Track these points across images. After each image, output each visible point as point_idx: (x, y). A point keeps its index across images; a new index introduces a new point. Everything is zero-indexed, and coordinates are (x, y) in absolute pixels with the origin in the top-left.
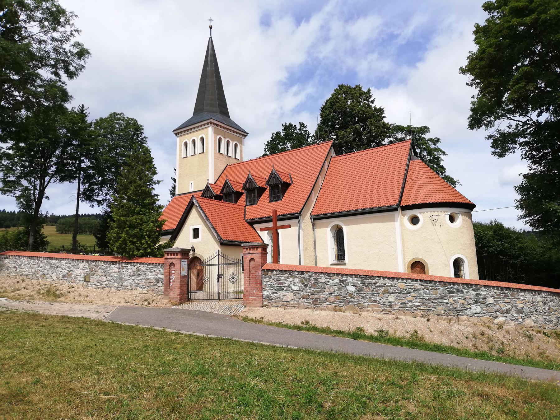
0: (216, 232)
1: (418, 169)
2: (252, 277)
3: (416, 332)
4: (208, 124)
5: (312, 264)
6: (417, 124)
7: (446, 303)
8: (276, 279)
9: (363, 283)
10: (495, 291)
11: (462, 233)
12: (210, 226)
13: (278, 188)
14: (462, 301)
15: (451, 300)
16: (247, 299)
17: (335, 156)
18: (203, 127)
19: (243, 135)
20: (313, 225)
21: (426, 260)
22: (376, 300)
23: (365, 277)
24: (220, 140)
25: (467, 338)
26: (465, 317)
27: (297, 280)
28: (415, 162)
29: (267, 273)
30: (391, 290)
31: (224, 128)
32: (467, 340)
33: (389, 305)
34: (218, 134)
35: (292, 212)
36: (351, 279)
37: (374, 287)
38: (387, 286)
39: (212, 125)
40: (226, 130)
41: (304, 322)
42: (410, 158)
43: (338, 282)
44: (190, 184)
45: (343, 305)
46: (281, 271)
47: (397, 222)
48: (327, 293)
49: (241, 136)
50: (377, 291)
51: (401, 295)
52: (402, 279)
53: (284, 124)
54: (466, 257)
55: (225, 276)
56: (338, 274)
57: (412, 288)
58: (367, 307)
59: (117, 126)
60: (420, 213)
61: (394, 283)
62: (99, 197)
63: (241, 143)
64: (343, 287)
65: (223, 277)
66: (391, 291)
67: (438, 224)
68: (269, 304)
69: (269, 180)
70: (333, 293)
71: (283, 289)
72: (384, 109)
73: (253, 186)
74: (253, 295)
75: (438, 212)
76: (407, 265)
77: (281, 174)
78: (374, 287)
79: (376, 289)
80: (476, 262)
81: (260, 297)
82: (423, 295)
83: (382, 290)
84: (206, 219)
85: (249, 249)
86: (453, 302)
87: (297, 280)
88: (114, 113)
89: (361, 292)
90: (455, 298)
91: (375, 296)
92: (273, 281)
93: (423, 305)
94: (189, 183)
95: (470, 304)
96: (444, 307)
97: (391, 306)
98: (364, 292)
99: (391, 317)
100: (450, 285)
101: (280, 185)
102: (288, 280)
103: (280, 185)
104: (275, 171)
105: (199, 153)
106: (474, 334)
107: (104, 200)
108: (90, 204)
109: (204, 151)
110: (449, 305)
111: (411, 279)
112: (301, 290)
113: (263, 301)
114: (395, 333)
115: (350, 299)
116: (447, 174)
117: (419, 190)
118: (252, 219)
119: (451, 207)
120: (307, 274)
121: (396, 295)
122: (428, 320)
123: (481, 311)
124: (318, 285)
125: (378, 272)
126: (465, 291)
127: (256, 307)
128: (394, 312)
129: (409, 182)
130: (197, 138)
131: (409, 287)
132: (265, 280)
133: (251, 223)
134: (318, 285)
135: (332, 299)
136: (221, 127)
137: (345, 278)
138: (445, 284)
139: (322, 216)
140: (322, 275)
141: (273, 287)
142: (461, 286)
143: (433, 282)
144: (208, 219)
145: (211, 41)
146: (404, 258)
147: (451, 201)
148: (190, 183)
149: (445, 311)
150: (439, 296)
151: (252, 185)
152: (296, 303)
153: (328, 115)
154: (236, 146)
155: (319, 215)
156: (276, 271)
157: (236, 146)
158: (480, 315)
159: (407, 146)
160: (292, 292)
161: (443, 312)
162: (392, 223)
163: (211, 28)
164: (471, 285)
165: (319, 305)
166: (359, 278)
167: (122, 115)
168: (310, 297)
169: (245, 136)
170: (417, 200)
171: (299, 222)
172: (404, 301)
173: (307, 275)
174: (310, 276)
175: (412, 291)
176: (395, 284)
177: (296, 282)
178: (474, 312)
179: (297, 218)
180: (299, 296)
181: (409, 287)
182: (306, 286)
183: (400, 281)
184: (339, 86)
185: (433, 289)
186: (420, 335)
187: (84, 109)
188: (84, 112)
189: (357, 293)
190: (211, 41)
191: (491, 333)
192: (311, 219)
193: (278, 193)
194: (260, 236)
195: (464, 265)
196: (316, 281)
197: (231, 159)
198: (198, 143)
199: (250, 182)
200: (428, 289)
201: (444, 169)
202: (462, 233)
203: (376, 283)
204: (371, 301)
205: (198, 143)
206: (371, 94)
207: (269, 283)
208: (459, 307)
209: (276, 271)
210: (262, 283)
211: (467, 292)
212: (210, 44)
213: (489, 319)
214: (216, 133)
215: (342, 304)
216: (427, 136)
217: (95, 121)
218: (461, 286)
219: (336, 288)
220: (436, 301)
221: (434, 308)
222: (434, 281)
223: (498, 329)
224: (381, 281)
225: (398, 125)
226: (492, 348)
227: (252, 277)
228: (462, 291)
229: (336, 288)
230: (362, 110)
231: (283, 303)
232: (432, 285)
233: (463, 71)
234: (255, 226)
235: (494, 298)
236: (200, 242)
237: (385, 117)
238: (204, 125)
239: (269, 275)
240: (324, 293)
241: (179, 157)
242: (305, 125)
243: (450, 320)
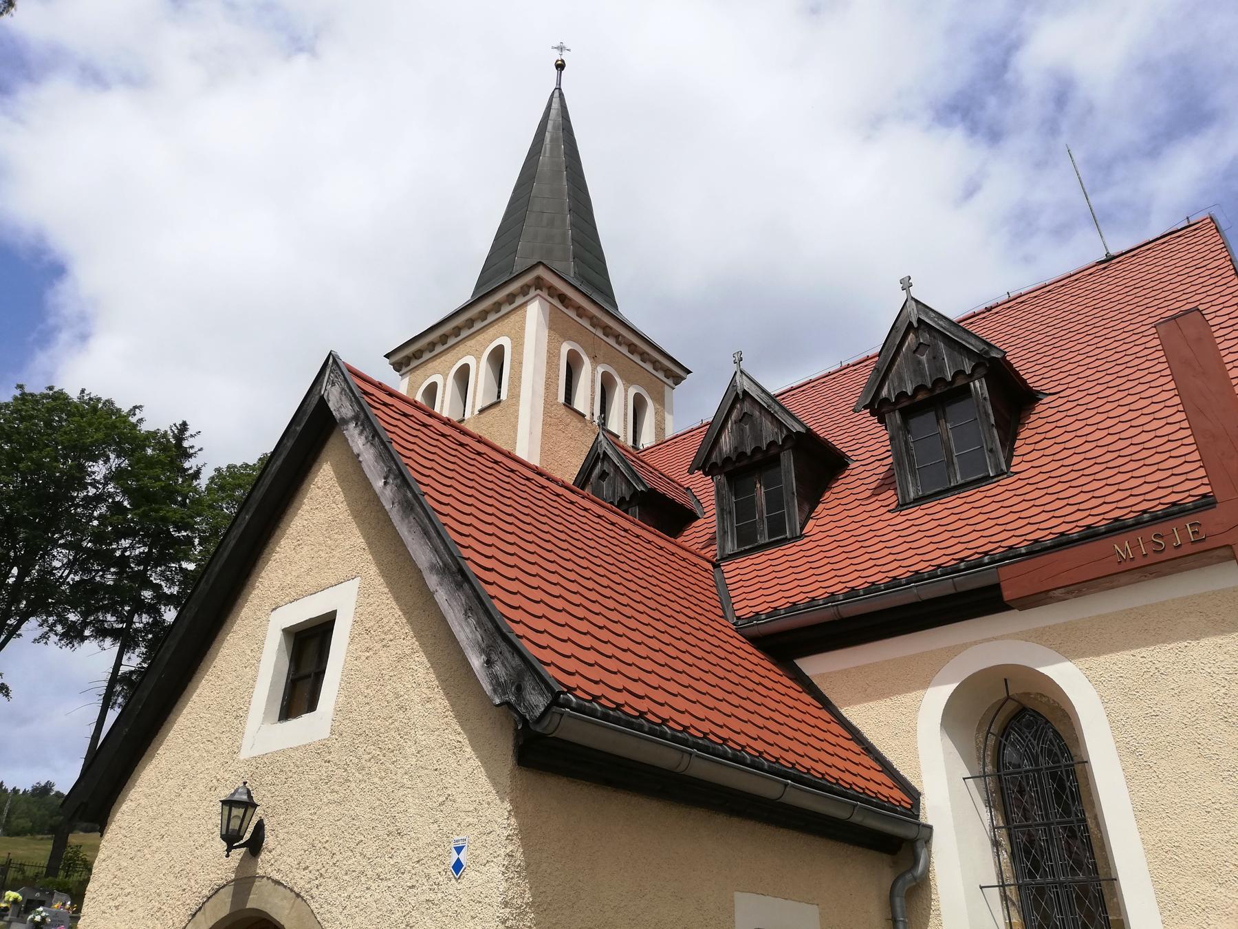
0: (479, 606)
4: (524, 291)
19: (668, 373)
39: (545, 294)
40: (600, 333)
49: (660, 375)
63: (660, 400)
73: (769, 432)
105: (478, 407)
109: (504, 396)
130: (478, 359)
136: (580, 311)
144: (412, 503)
151: (757, 435)
163: (560, 66)
169: (678, 380)
187: (187, 434)
188: (186, 444)
194: (869, 749)
198: (480, 374)
214: (557, 328)
217: (213, 473)
234: (813, 666)
236: (321, 750)
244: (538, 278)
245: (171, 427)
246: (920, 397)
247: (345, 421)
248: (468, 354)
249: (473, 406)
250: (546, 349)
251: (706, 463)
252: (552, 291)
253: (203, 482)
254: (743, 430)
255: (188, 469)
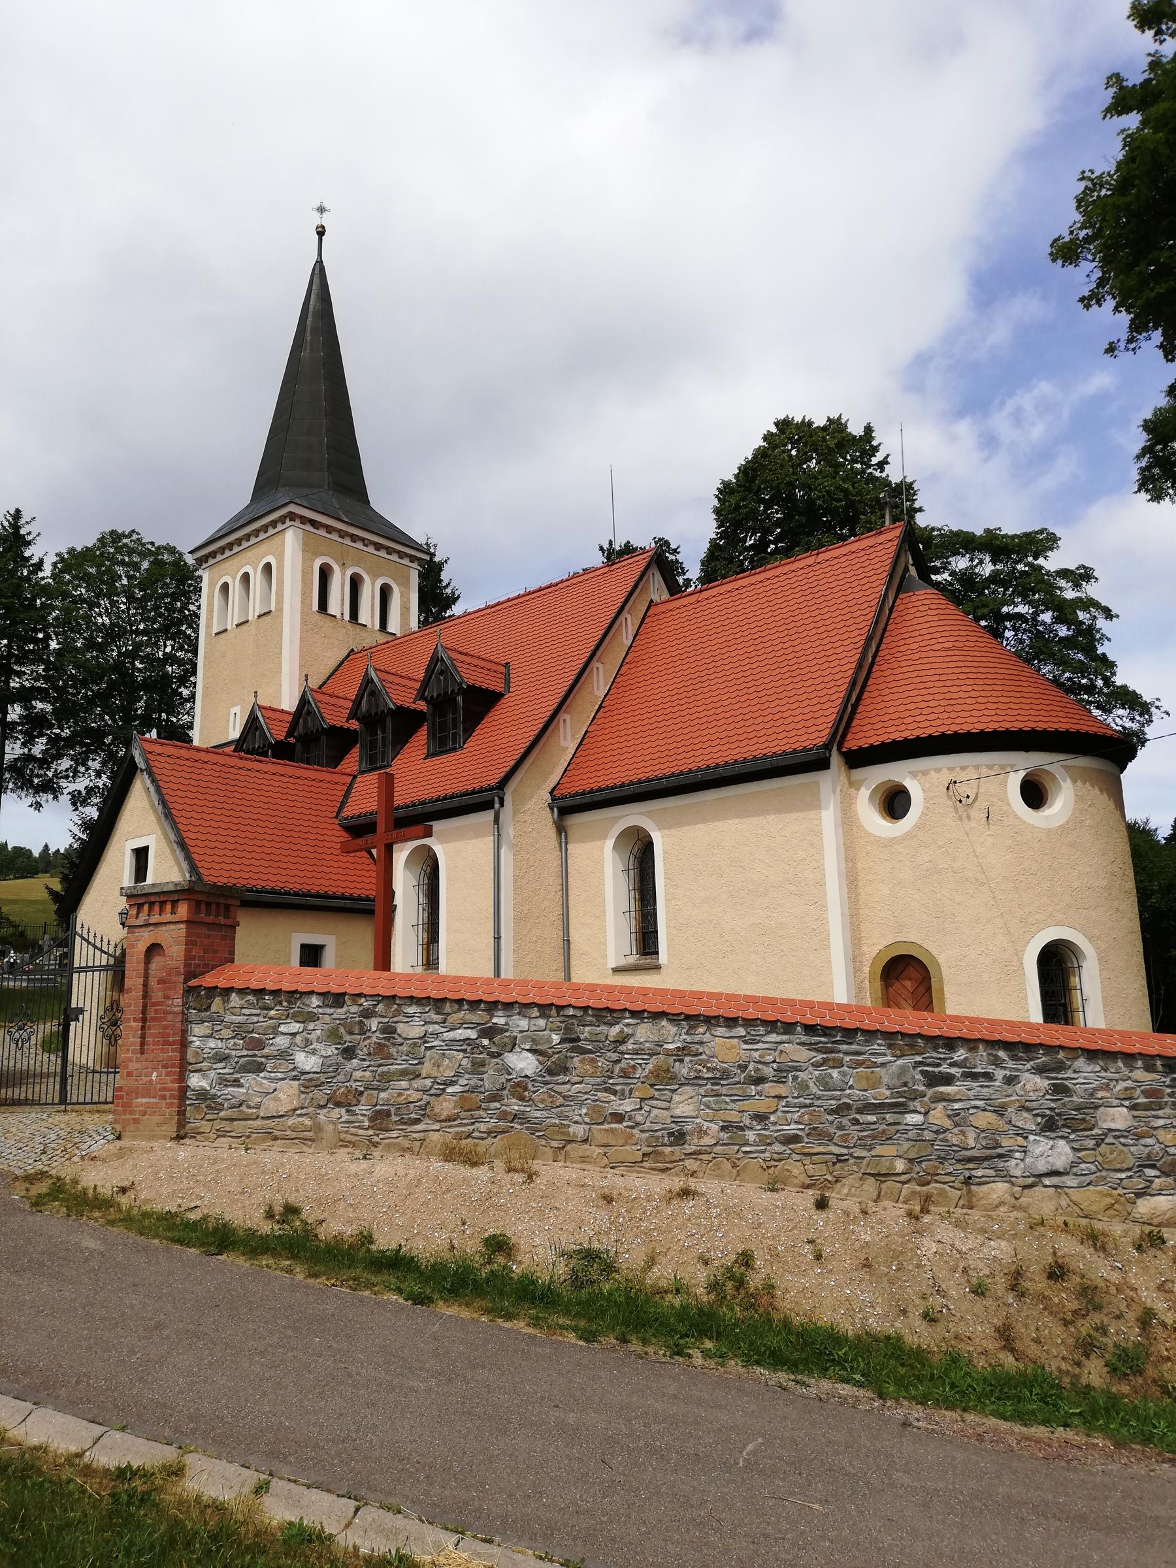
1: (921, 620)
2: (154, 1019)
3: (746, 1259)
4: (282, 520)
5: (548, 972)
6: (1012, 526)
7: (916, 1126)
8: (240, 1026)
9: (571, 1039)
10: (1140, 1074)
11: (1072, 845)
12: (172, 837)
13: (455, 711)
14: (984, 1119)
15: (938, 1115)
16: (127, 1106)
17: (666, 596)
18: (271, 531)
20: (561, 829)
21: (934, 952)
22: (620, 1110)
23: (579, 1013)
24: (325, 574)
25: (979, 1291)
26: (1001, 1187)
27: (317, 1030)
28: (914, 598)
29: (205, 1002)
30: (683, 1070)
31: (343, 534)
32: (979, 1305)
33: (671, 1134)
34: (317, 554)
35: (477, 786)
36: (524, 1023)
37: (615, 1057)
38: (668, 1053)
39: (297, 523)
40: (348, 541)
41: (278, 1209)
42: (898, 584)
43: (473, 1034)
44: (232, 716)
45: (489, 1133)
46: (259, 993)
47: (827, 808)
48: (428, 1082)
49: (406, 562)
50: (625, 1074)
51: (724, 1090)
52: (731, 1022)
53: (606, 546)
54: (1091, 939)
55: (87, 1015)
56: (475, 1004)
57: (769, 1058)
58: (585, 1141)
59: (120, 570)
60: (914, 774)
61: (697, 1038)
62: (78, 780)
64: (492, 1055)
65: (81, 1017)
66: (685, 1071)
67: (978, 813)
68: (205, 1126)
69: (425, 683)
70: (452, 1083)
71: (260, 1068)
72: (916, 486)
74: (147, 1091)
75: (977, 767)
76: (866, 969)
77: (468, 659)
78: (615, 1057)
79: (623, 1064)
80: (1139, 959)
81: (172, 1097)
82: (814, 1089)
83: (650, 1066)
84: (168, 813)
85: (146, 907)
86: (948, 1123)
87: (317, 1030)
88: (113, 532)
89: (561, 1078)
90: (956, 1106)
91: (615, 1093)
92: (227, 1033)
93: (816, 1133)
94: (229, 714)
95: (1023, 1134)
96: (906, 1145)
97: (679, 1138)
98: (577, 1079)
99: (659, 1184)
100: (935, 1049)
101: (459, 699)
102: (282, 1029)
103: (459, 699)
104: (445, 648)
106: (1018, 1274)
107: (90, 791)
108: (30, 800)
110: (928, 1135)
111: (764, 1022)
112: (330, 1070)
113: (182, 1113)
114: (651, 1261)
115: (515, 1106)
116: (1119, 680)
117: (911, 693)
118: (359, 816)
119: (1027, 749)
120: (355, 1002)
121: (702, 1091)
122: (822, 1204)
123: (1073, 1164)
124: (393, 1050)
125: (753, 1000)
126: (1000, 1074)
127: (153, 1138)
128: (691, 1164)
129: (883, 668)
130: (255, 570)
131: (756, 1055)
132: (198, 1029)
133: (360, 829)
134: (393, 1050)
135: (446, 1106)
136: (329, 529)
137: (499, 1020)
138: (912, 1046)
139: (586, 799)
140: (411, 1010)
141: (226, 1058)
142: (982, 1051)
143: (859, 1037)
145: (319, 271)
146: (855, 941)
147: (1027, 726)
148: (233, 710)
149: (910, 1161)
150: (883, 1094)
151: (377, 707)
152: (307, 1122)
153: (737, 508)
154: (385, 592)
155: (577, 794)
156: (242, 992)
157: (385, 592)
158: (1069, 1181)
159: (890, 544)
160: (294, 1078)
161: (900, 1166)
162: (812, 814)
163: (321, 232)
164: (1028, 1047)
165: (394, 1134)
166: (556, 1021)
167: (135, 537)
168: (363, 1099)
170: (903, 727)
171: (497, 820)
172: (733, 1116)
173: (354, 1009)
174: (368, 1014)
175: (768, 1071)
176: (701, 1043)
177: (313, 1037)
178: (1042, 1167)
179: (486, 805)
180: (320, 1096)
181: (756, 1055)
182: (349, 1053)
183: (721, 1031)
184: (777, 424)
185: (859, 1064)
186: (755, 1281)
187: (22, 521)
188: (23, 531)
189: (546, 1083)
190: (319, 271)
191: (1101, 1270)
192: (552, 809)
193: (455, 727)
195: (1084, 971)
196: (389, 1030)
197: (364, 634)
199: (373, 693)
200: (839, 1064)
201: (1111, 665)
202: (1072, 845)
203: (622, 1040)
204: (601, 1116)
205: (257, 579)
206: (874, 443)
207: (212, 1043)
208: (971, 1142)
209: (242, 992)
210: (184, 1044)
211: (1010, 1081)
212: (316, 279)
213: (1109, 1200)
214: (309, 550)
215: (483, 1127)
216: (1052, 562)
217: (55, 559)
218: (982, 1051)
219: (464, 1062)
220: (872, 1118)
221: (863, 1146)
222: (864, 1032)
223: (1139, 1248)
224: (644, 1032)
225: (955, 529)
226: (1087, 1347)
227: (154, 1019)
228: (988, 1076)
229: (464, 1062)
230: (839, 488)
231: (259, 1123)
232: (855, 1047)
233: (1066, 252)
235: (1133, 1107)
237: (920, 510)
238: (274, 524)
239: (214, 1008)
240: (417, 1083)
241: (207, 633)
242: (673, 546)
243: (926, 1203)
244: (290, 512)
245: (5, 516)
246: (440, 699)
247: (142, 771)
248: (248, 564)
249: (254, 611)
250: (301, 569)
251: (353, 714)
252: (304, 520)
253: (47, 571)
254: (371, 700)
255: (31, 557)
